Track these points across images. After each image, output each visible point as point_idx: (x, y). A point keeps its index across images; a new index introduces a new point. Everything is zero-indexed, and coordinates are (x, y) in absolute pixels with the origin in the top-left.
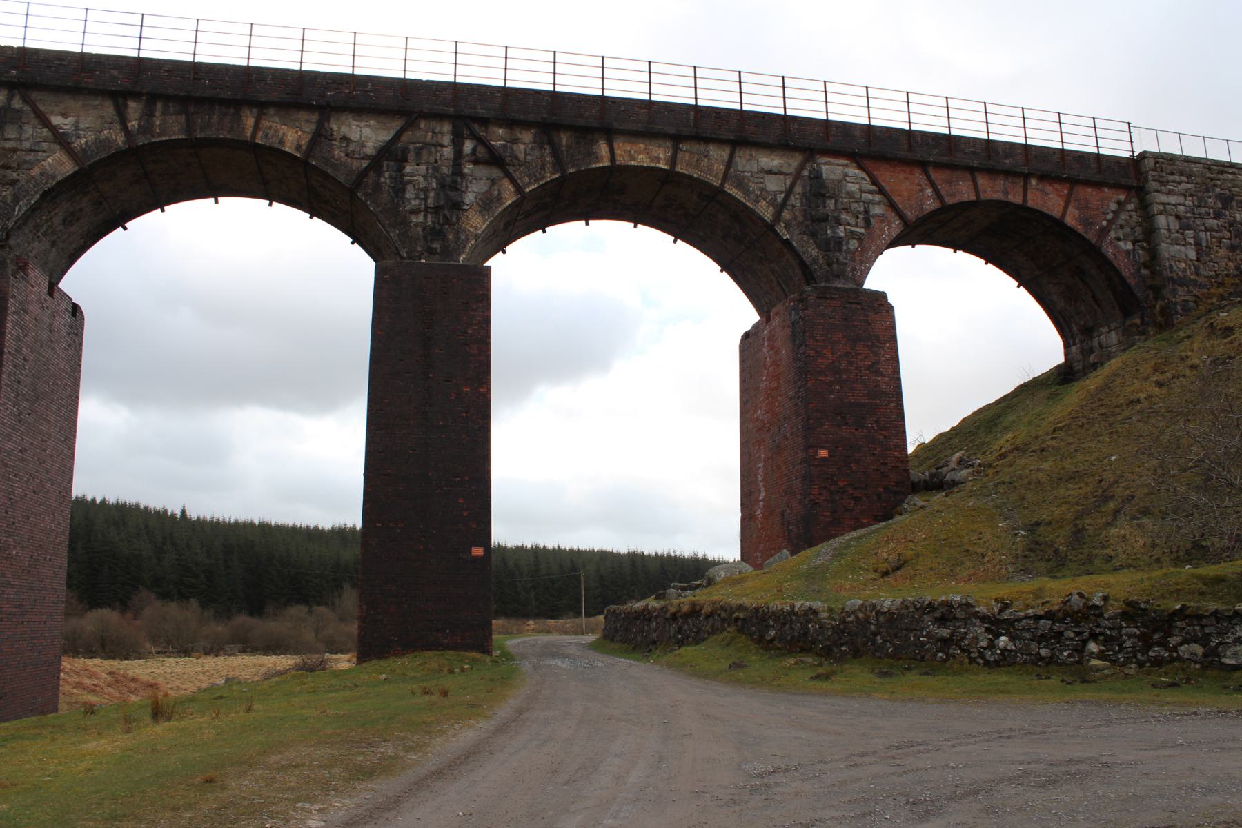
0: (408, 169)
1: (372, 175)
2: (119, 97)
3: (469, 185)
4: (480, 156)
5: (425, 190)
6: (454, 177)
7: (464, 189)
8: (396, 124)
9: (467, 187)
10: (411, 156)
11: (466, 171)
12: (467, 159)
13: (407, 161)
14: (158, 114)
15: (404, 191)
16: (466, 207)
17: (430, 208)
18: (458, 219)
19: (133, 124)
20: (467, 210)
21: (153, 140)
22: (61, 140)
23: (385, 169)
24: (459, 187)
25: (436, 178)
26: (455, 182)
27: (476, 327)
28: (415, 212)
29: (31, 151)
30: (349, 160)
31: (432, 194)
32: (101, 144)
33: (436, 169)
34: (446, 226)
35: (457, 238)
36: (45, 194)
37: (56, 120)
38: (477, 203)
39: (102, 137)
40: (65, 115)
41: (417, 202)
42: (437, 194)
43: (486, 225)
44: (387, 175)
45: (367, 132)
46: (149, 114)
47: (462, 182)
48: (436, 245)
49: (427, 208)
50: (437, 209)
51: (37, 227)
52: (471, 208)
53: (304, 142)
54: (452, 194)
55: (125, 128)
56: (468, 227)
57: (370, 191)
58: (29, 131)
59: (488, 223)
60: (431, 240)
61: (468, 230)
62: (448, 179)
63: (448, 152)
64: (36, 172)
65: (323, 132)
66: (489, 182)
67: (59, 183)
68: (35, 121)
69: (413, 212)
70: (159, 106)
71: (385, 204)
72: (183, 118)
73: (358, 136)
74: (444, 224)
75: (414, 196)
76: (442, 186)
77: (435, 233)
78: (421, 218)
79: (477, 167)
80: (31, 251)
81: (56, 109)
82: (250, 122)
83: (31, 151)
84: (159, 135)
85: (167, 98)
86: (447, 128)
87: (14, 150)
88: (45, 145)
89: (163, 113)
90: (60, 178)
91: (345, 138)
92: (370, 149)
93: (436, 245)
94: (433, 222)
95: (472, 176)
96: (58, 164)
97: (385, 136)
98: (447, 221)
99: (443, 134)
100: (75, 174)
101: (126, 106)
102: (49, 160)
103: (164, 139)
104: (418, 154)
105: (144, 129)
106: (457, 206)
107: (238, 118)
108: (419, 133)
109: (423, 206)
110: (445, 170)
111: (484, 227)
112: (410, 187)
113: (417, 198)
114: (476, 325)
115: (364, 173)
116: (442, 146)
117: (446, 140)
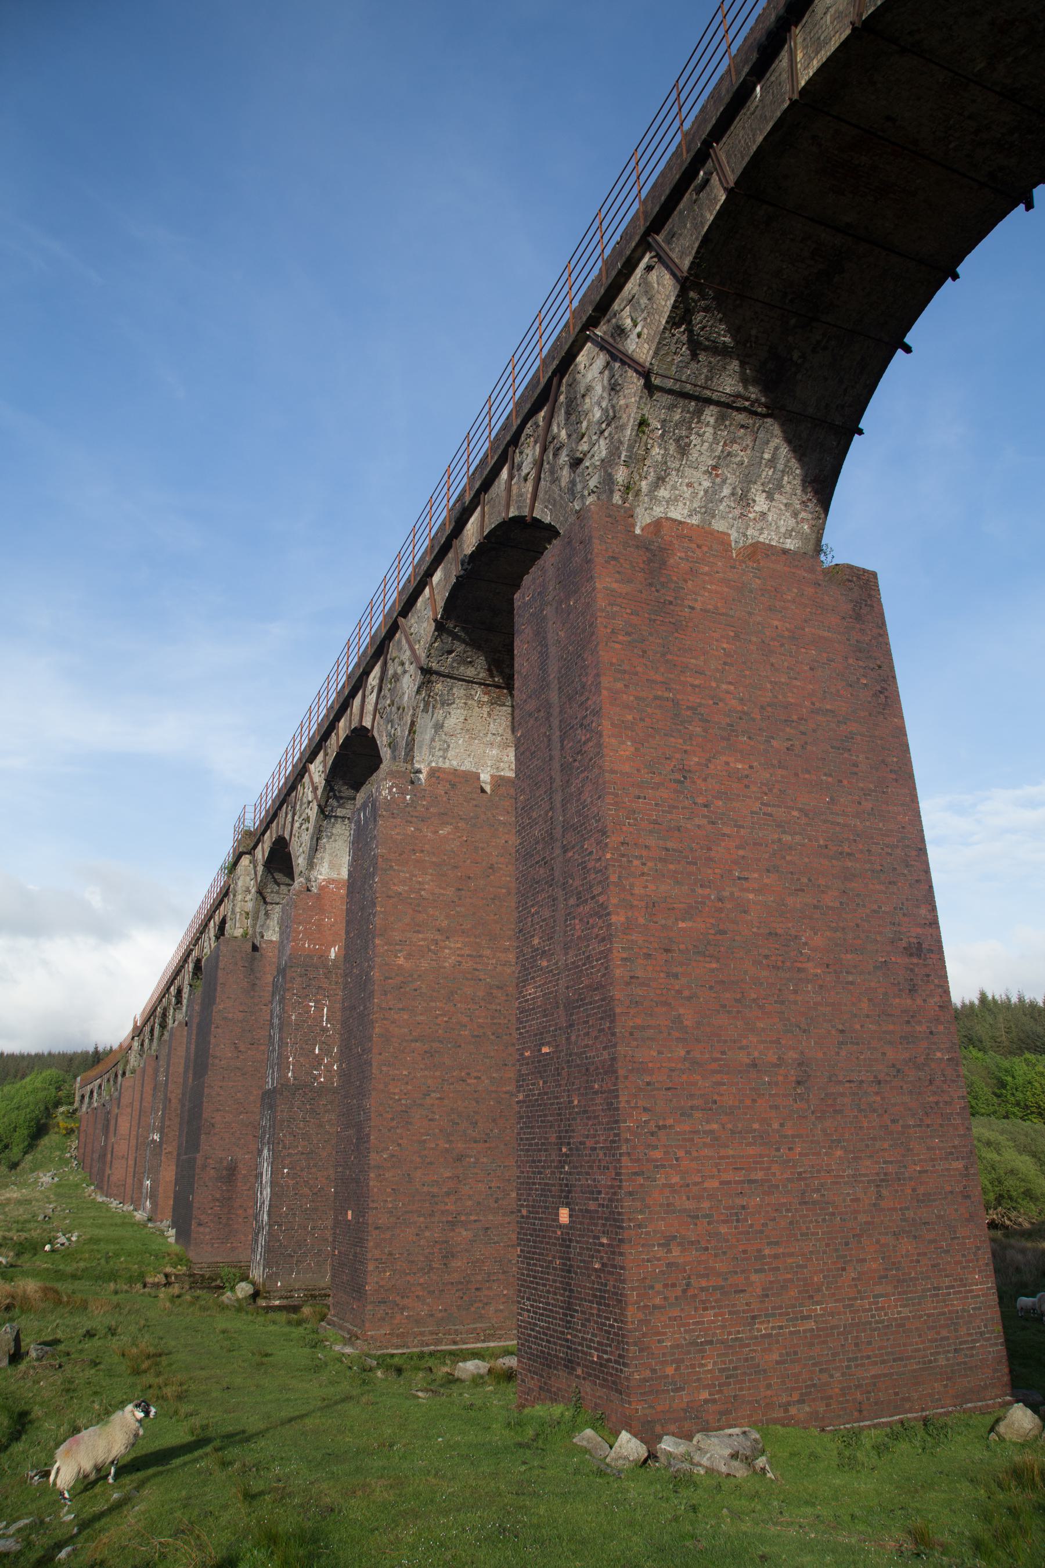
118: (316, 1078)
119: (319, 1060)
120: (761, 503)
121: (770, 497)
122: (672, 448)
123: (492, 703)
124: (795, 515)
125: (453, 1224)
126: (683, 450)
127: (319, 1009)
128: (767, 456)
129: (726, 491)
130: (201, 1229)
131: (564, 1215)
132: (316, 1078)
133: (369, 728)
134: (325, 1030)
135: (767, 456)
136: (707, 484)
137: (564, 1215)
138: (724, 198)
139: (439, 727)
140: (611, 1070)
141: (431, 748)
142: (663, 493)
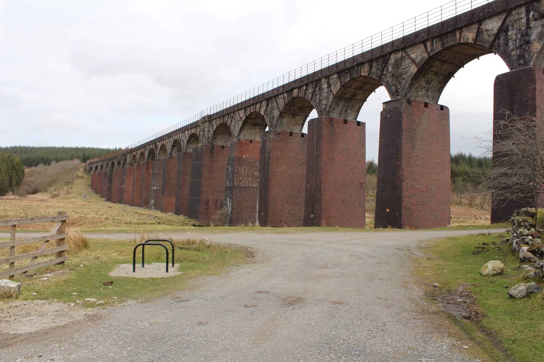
0: (509, 33)
1: (497, 40)
2: (424, 42)
3: (533, 31)
4: (536, 17)
5: (516, 40)
6: (527, 30)
7: (531, 34)
8: (503, 17)
9: (532, 32)
10: (510, 28)
11: (532, 25)
12: (532, 20)
13: (508, 30)
14: (434, 43)
15: (508, 43)
16: (532, 41)
17: (518, 47)
18: (529, 48)
19: (429, 50)
20: (533, 42)
21: (435, 53)
22: (413, 61)
23: (501, 37)
24: (529, 34)
25: (520, 33)
26: (527, 32)
27: (531, 93)
28: (512, 51)
29: (408, 67)
30: (489, 38)
31: (518, 41)
32: (422, 59)
33: (520, 30)
34: (525, 52)
35: (529, 56)
36: (412, 79)
37: (412, 56)
38: (537, 38)
39: (422, 57)
40: (414, 53)
41: (513, 46)
42: (520, 40)
43: (541, 46)
44: (502, 39)
45: (494, 24)
46: (432, 44)
47: (530, 31)
48: (521, 62)
49: (516, 47)
50: (520, 46)
51: (417, 88)
52: (534, 41)
53: (474, 37)
54: (525, 38)
55: (427, 52)
56: (533, 50)
57: (496, 47)
58: (406, 61)
59: (542, 45)
60: (519, 60)
61: (534, 51)
62: (524, 32)
63: (524, 21)
64: (409, 74)
65: (480, 31)
66: (542, 26)
67: (415, 75)
68: (408, 58)
69: (512, 51)
70: (435, 40)
71: (502, 51)
72: (440, 43)
73: (491, 27)
74: (523, 52)
75: (512, 44)
76: (522, 36)
77: (521, 57)
78: (515, 52)
79: (536, 21)
80: (419, 95)
81: (412, 52)
82: (458, 36)
83: (408, 67)
84: (436, 50)
85: (436, 37)
86: (523, 9)
87: (404, 68)
88: (410, 64)
89: (436, 43)
90: (414, 74)
91: (487, 30)
92: (495, 31)
93: (521, 62)
94: (520, 52)
95: (534, 27)
96: (413, 69)
97: (500, 24)
98: (525, 50)
99: (521, 13)
100: (418, 71)
101: (427, 44)
102: (412, 69)
103: (437, 51)
104: (513, 26)
105: (432, 50)
106: (528, 42)
107: (455, 35)
108: (512, 17)
109: (515, 47)
110: (523, 29)
111: (540, 48)
112: (510, 41)
113: (513, 44)
114: (530, 92)
115: (494, 41)
116: (522, 18)
117: (523, 15)
118: (241, 184)
119: (241, 181)
120: (349, 111)
121: (351, 110)
122: (336, 105)
123: (292, 118)
124: (354, 112)
125: (282, 216)
126: (338, 105)
127: (241, 169)
128: (351, 105)
129: (344, 110)
130: (201, 215)
131: (312, 216)
132: (241, 184)
133: (263, 115)
134: (242, 174)
135: (351, 105)
136: (341, 109)
137: (312, 216)
138: (349, 79)
139: (282, 122)
140: (321, 199)
141: (280, 126)
142: (334, 111)
